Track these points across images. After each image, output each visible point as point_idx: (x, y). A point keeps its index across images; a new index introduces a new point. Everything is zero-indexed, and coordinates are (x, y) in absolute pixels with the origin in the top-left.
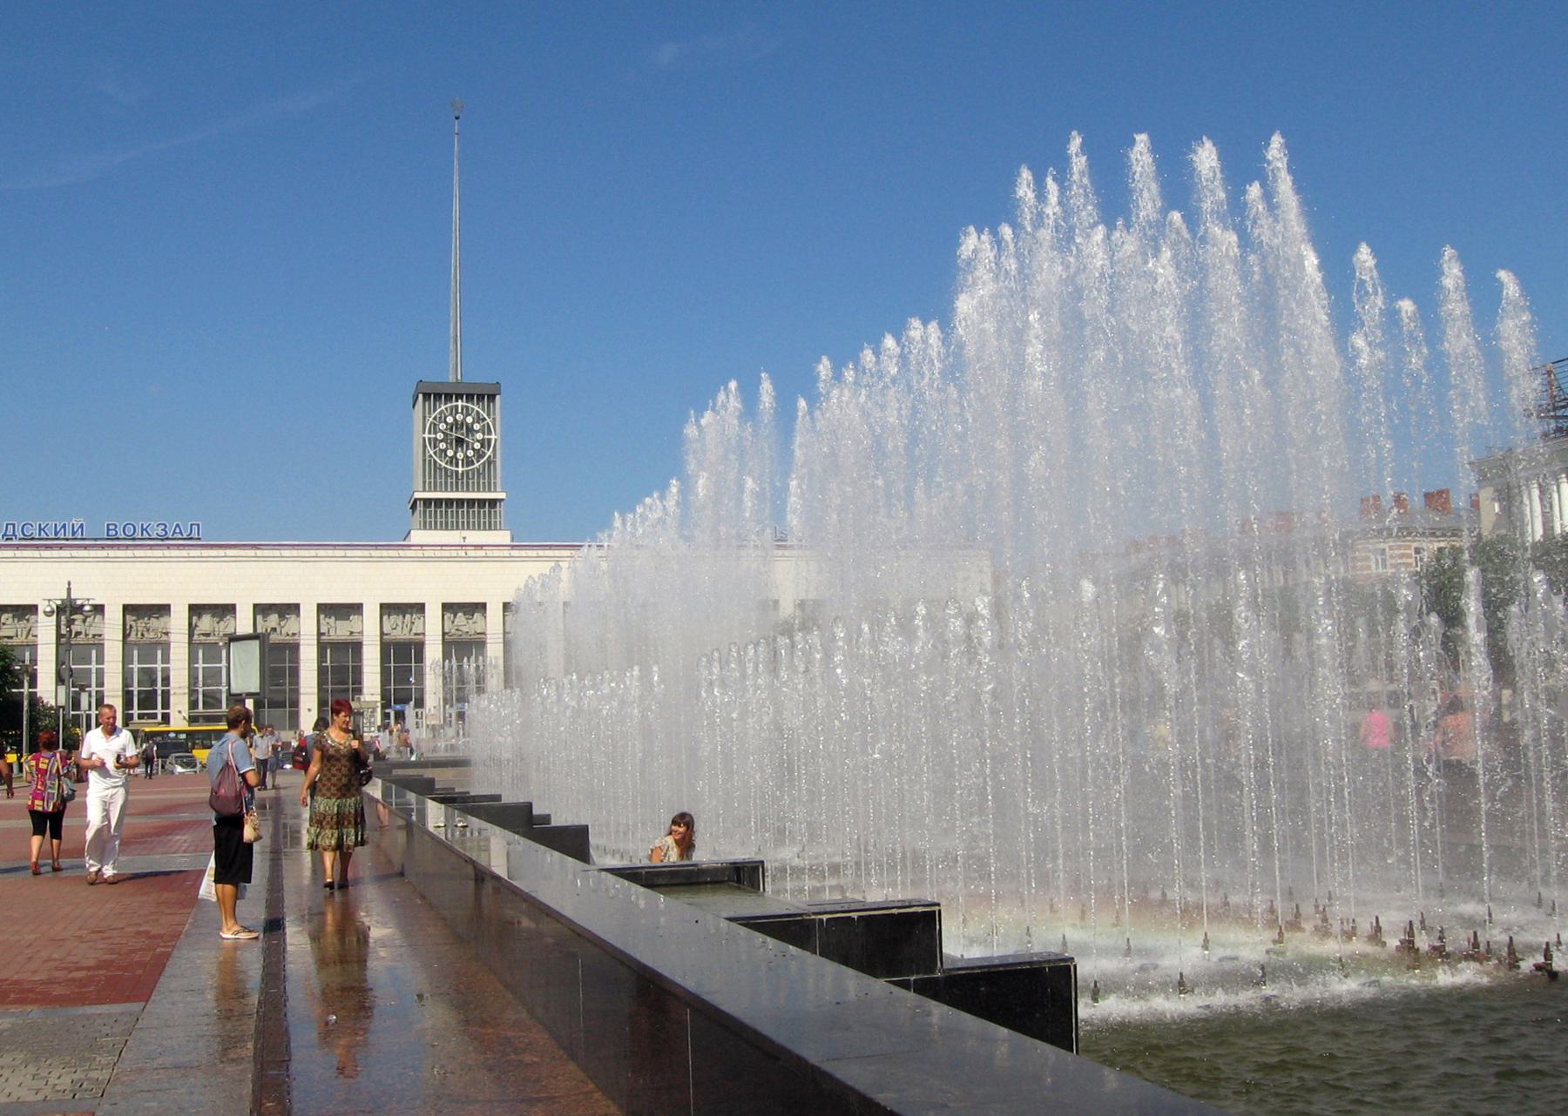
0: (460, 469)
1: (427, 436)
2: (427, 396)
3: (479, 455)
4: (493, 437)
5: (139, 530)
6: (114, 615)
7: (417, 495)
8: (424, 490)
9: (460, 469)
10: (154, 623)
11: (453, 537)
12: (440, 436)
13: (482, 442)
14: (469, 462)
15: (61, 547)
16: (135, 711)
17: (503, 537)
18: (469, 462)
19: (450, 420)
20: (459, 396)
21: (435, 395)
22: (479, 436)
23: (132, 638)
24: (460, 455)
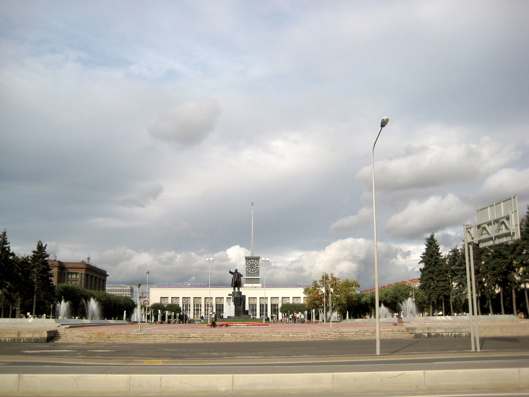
0: (253, 273)
1: (247, 266)
2: (246, 259)
3: (256, 270)
4: (259, 266)
5: (196, 284)
6: (192, 299)
7: (245, 277)
8: (246, 276)
9: (253, 273)
10: (199, 301)
11: (251, 285)
12: (249, 266)
13: (256, 267)
14: (254, 271)
15: (183, 287)
16: (195, 316)
17: (260, 285)
18: (254, 271)
19: (251, 263)
20: (252, 259)
21: (248, 259)
22: (256, 266)
23: (195, 303)
24: (253, 270)
